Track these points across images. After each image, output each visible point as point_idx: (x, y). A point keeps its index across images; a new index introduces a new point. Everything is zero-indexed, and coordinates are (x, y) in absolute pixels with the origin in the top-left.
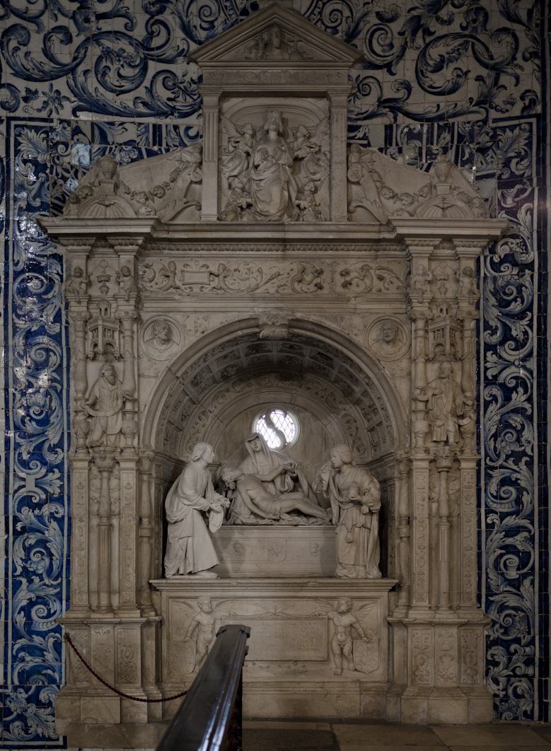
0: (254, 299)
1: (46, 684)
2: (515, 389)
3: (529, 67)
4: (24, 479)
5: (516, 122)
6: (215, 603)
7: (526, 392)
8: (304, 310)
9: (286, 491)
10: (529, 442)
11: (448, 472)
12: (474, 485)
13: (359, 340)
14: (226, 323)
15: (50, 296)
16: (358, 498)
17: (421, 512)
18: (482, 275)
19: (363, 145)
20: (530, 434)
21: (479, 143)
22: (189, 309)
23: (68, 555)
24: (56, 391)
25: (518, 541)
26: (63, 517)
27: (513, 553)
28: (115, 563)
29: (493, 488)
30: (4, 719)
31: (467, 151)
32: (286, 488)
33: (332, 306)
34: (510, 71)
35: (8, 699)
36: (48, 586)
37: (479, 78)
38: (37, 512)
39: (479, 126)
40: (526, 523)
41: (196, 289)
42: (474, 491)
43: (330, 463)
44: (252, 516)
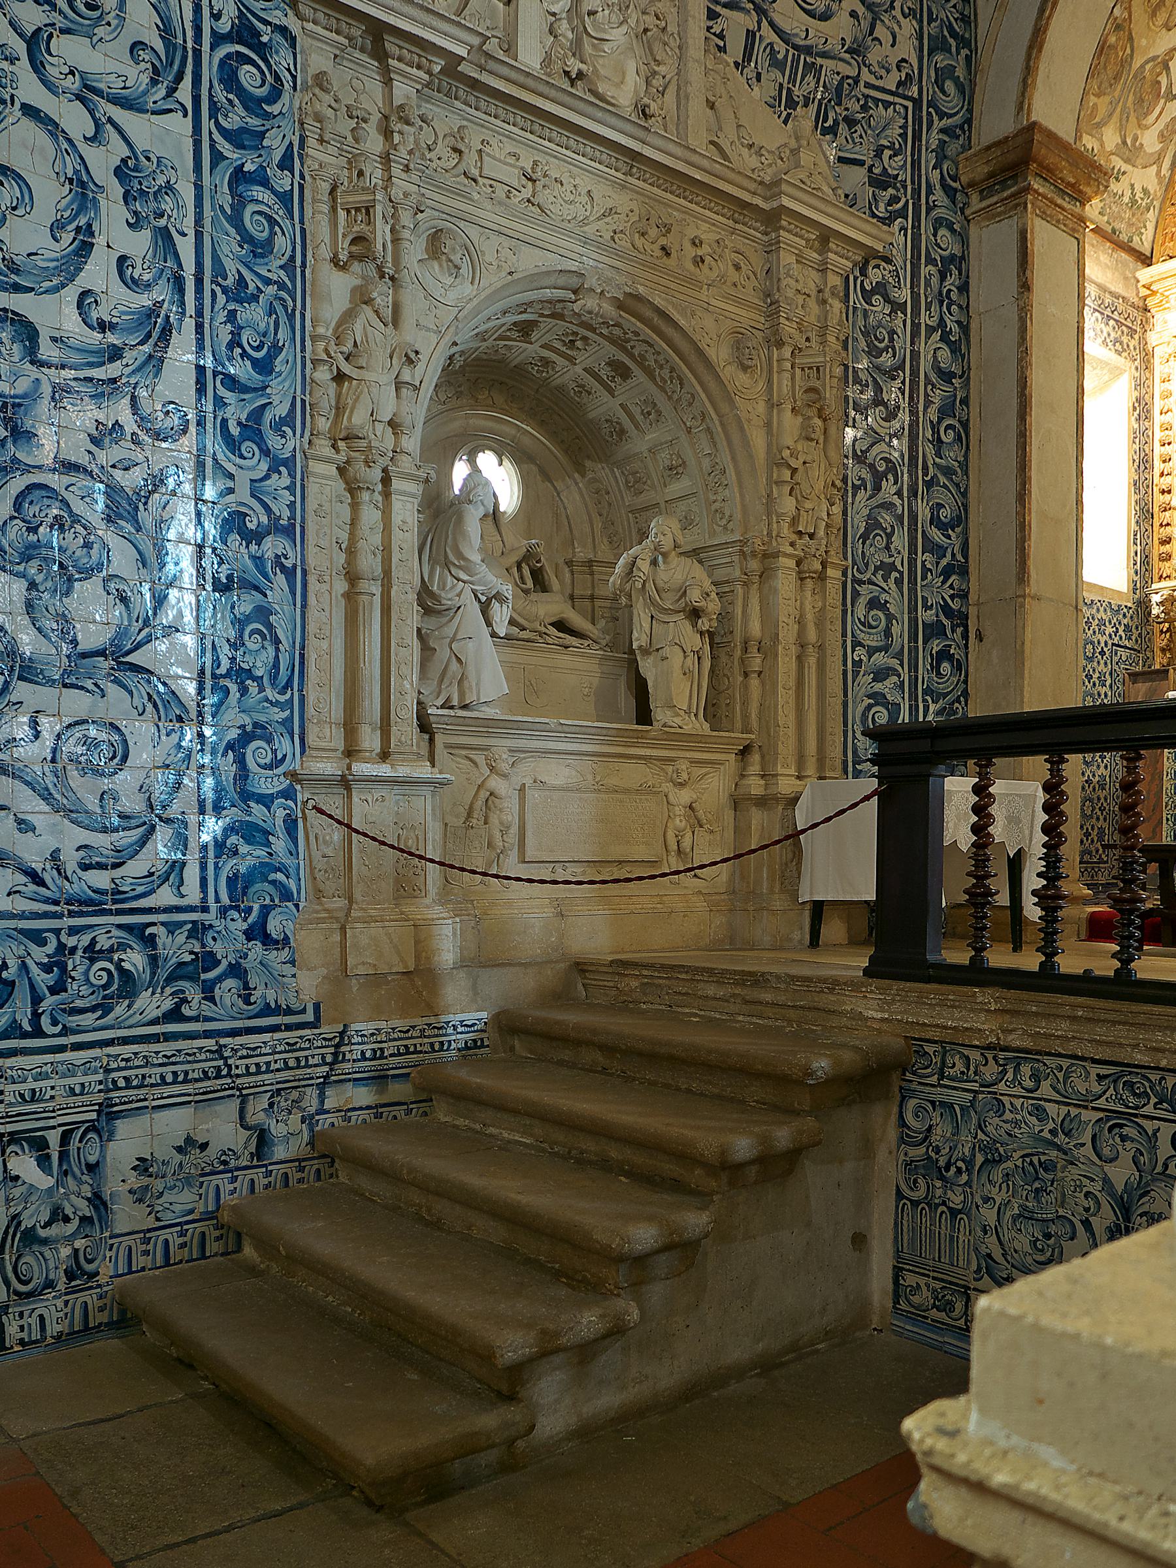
1: (277, 901)
3: (908, 27)
4: (231, 477)
5: (890, 98)
7: (896, 483)
10: (899, 553)
12: (839, 603)
13: (711, 353)
15: (275, 109)
18: (851, 303)
19: (720, 49)
20: (900, 541)
21: (847, 109)
22: (491, 225)
23: (303, 648)
24: (285, 308)
25: (886, 687)
26: (295, 566)
27: (882, 705)
29: (861, 611)
30: (203, 976)
31: (831, 115)
34: (887, 21)
35: (211, 934)
36: (271, 703)
37: (853, 14)
38: (253, 547)
39: (849, 85)
40: (895, 663)
41: (501, 191)
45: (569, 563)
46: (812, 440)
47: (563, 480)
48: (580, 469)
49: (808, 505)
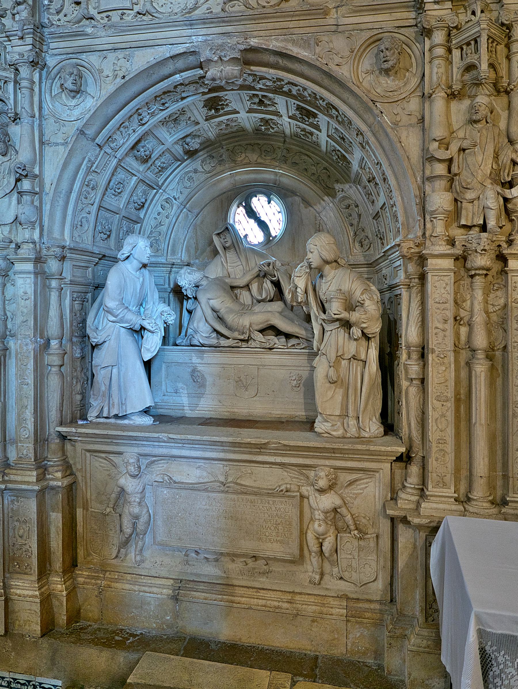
0: (191, 24)
6: (144, 462)
8: (262, 33)
9: (263, 301)
11: (486, 275)
14: (155, 62)
16: (344, 315)
17: (441, 341)
32: (264, 296)
33: (302, 23)
43: (305, 263)
44: (214, 335)
46: (479, 121)
47: (320, 203)
48: (330, 192)
49: (470, 195)
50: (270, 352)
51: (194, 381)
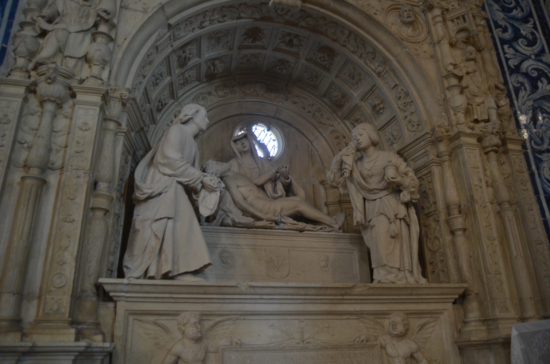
2: (538, 78)
12: (525, 169)
28: (42, 245)
42: (526, 175)
45: (322, 183)
50: (301, 234)
51: (224, 262)
